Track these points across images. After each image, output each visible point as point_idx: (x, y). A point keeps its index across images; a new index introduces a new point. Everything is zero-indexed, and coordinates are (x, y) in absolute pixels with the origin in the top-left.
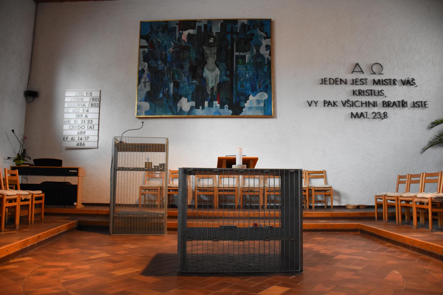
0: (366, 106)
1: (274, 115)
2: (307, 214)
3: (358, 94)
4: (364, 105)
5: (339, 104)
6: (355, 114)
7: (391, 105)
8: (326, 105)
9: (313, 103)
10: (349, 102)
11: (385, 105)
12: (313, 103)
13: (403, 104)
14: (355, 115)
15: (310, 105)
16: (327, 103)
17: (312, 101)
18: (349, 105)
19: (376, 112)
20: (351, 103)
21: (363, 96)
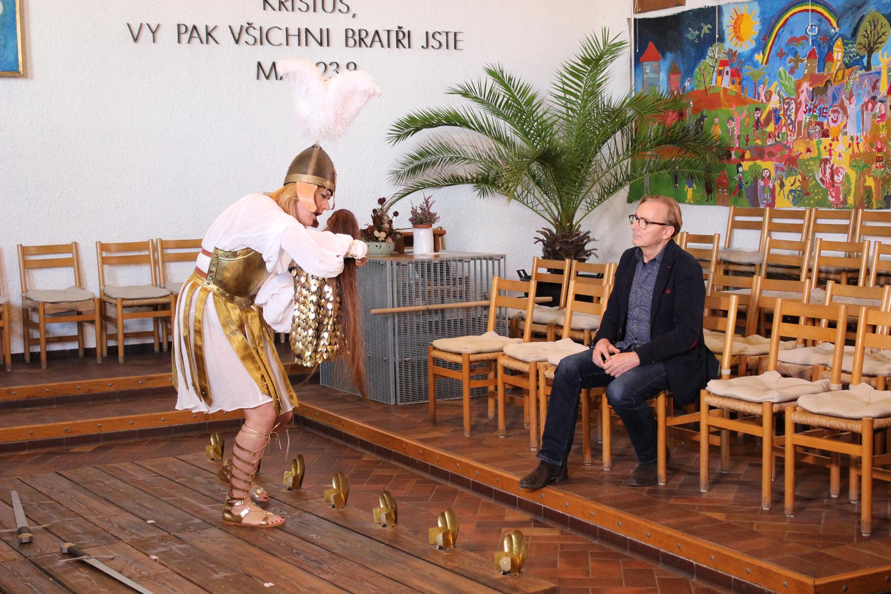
0: (299, 44)
1: (25, 67)
2: (150, 379)
3: (276, 6)
4: (294, 40)
5: (223, 35)
6: (267, 67)
7: (368, 41)
8: (185, 38)
9: (146, 29)
10: (251, 31)
11: (351, 42)
12: (146, 29)
13: (402, 38)
14: (267, 73)
15: (136, 40)
16: (188, 33)
17: (141, 25)
18: (251, 41)
19: (328, 63)
20: (257, 34)
21: (291, 13)
